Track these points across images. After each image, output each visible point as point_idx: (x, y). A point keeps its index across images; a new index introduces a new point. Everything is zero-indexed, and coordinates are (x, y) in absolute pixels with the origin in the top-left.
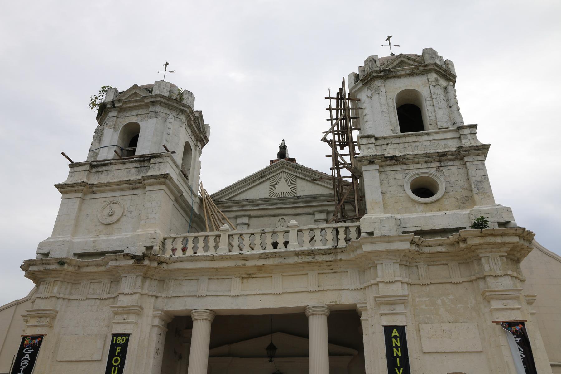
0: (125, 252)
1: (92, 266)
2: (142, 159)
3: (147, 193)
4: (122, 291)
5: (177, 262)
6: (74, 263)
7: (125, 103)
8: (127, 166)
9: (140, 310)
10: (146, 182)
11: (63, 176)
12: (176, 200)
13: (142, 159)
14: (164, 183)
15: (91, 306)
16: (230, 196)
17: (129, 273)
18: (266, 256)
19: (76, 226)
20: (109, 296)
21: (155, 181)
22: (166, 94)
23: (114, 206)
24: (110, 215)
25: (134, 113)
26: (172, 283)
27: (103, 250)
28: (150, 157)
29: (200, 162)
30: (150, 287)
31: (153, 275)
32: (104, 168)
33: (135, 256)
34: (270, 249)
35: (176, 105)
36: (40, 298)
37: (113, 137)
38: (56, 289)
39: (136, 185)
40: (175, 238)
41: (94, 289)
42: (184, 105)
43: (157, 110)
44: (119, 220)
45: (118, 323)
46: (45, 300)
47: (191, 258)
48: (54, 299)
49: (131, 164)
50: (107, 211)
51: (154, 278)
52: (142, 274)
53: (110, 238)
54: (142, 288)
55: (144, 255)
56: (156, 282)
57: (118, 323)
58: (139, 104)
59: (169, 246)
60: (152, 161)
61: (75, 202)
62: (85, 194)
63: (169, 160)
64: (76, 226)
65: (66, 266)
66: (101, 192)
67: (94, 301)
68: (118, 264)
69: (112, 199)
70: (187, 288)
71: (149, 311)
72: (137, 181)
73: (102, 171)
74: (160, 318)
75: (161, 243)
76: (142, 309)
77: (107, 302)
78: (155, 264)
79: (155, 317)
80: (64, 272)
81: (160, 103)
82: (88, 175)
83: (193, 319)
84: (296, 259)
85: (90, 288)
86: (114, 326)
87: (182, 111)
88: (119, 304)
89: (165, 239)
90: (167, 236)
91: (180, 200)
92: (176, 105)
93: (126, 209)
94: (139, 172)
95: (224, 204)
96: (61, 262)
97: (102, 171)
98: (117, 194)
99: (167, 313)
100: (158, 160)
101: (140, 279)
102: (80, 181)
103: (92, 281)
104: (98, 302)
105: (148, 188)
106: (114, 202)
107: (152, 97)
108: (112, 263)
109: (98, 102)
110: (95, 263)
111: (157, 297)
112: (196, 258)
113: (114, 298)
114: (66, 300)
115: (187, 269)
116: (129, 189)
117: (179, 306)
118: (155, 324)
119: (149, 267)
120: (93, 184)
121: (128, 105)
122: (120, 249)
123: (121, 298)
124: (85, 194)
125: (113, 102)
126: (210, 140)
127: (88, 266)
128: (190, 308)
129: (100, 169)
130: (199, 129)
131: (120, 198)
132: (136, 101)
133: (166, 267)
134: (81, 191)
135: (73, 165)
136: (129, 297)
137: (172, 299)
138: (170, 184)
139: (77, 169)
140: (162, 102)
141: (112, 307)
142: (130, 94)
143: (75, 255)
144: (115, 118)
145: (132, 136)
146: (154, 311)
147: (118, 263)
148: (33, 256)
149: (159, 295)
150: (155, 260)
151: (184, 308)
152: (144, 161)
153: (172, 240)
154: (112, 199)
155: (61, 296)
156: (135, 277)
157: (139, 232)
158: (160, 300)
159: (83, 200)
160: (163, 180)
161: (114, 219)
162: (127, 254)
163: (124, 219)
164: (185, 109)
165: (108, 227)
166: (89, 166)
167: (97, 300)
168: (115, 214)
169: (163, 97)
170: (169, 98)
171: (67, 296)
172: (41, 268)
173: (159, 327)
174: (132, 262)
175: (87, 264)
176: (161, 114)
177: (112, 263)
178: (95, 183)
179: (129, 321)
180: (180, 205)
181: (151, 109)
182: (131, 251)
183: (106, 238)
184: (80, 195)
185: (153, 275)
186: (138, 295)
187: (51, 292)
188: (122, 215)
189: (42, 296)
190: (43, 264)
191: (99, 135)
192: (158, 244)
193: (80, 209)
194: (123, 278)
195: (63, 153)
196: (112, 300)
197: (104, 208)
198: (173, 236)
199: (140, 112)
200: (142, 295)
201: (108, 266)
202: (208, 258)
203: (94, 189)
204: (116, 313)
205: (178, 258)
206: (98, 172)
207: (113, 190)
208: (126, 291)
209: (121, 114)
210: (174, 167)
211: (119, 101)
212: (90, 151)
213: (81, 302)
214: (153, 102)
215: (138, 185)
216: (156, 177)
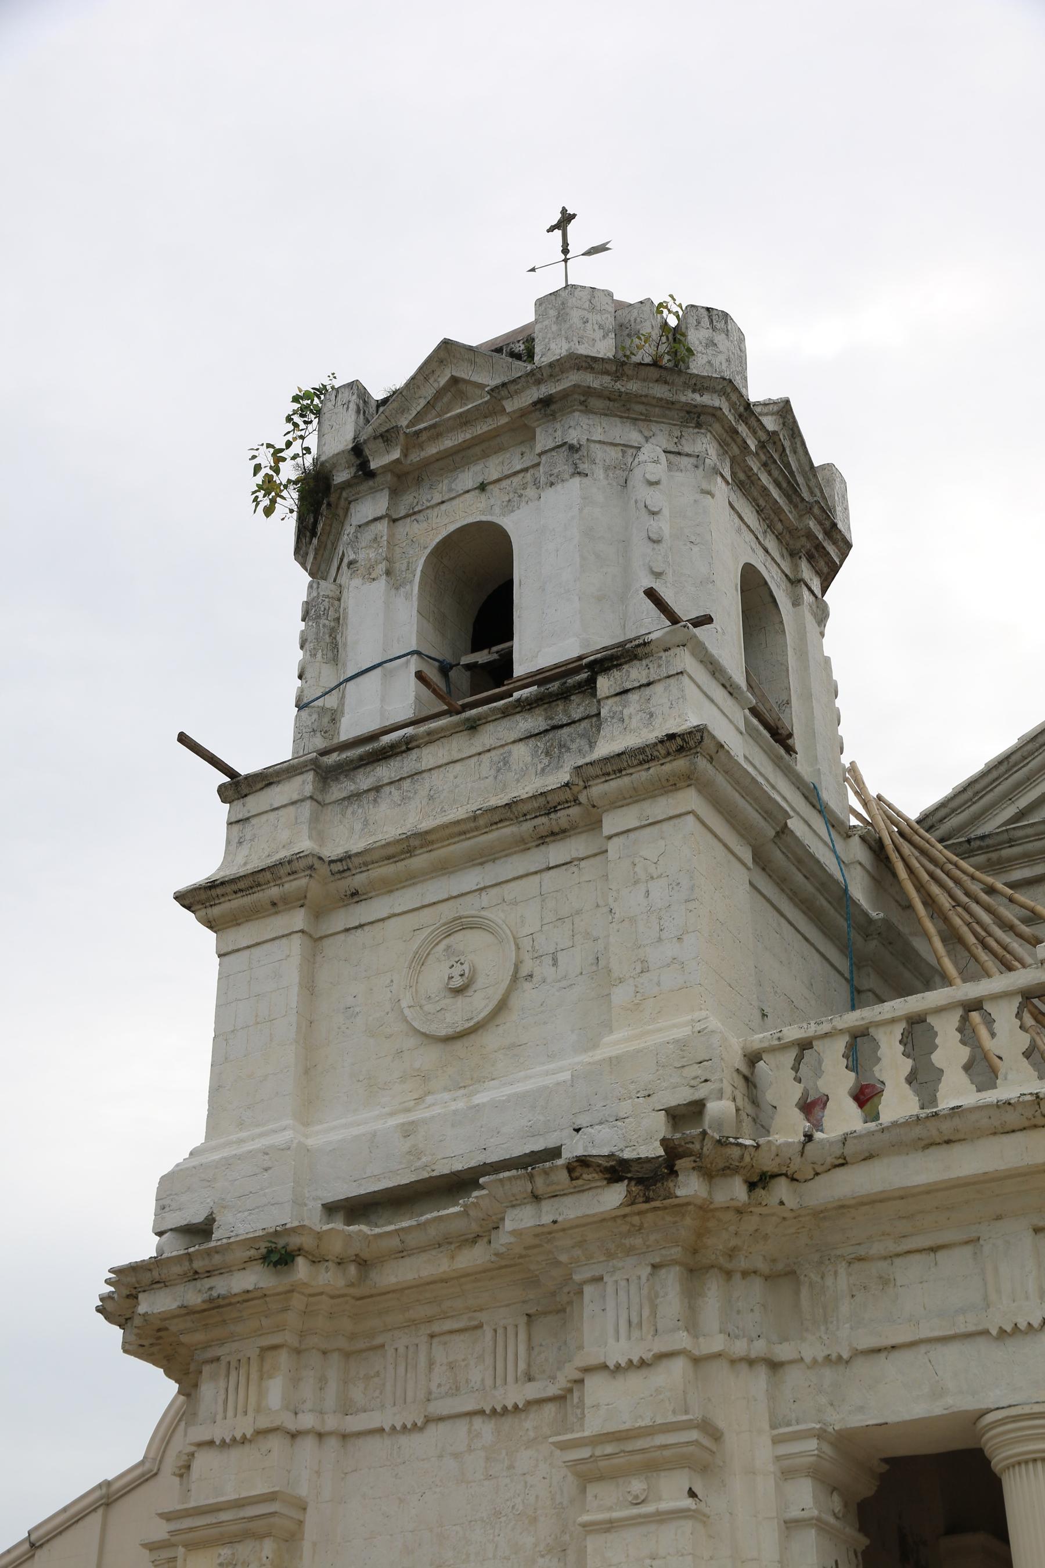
0: (567, 1155)
1: (422, 1249)
2: (554, 686)
3: (613, 846)
4: (592, 1355)
5: (843, 1163)
6: (336, 1247)
7: (414, 440)
8: (488, 736)
9: (706, 1442)
10: (598, 790)
11: (205, 851)
12: (761, 861)
13: (554, 686)
14: (688, 779)
15: (456, 1456)
16: (1023, 802)
17: (610, 1255)
19: (306, 1072)
20: (532, 1391)
21: (642, 776)
22: (604, 348)
23: (470, 941)
24: (459, 991)
25: (467, 479)
26: (841, 1280)
27: (458, 1166)
28: (591, 666)
29: (827, 661)
30: (729, 1316)
31: (732, 1253)
32: (384, 772)
33: (625, 1163)
35: (659, 391)
36: (211, 1443)
37: (392, 618)
38: (275, 1391)
39: (552, 820)
40: (804, 1046)
41: (451, 1366)
42: (701, 384)
43: (573, 436)
44: (502, 1006)
45: (609, 1526)
46: (235, 1453)
47: (917, 1131)
48: (275, 1443)
49: (506, 723)
50: (437, 974)
51: (743, 1264)
52: (676, 1252)
53: (481, 1098)
54: (691, 1324)
55: (673, 1152)
56: (757, 1285)
57: (609, 1526)
58: (482, 428)
59: (782, 1087)
60: (604, 684)
61: (280, 957)
62: (318, 914)
63: (685, 660)
64: (309, 1070)
65: (302, 1268)
67: (462, 1426)
68: (547, 1219)
69: (448, 911)
70: (926, 1294)
71: (752, 1446)
72: (554, 799)
73: (377, 789)
74: (816, 1474)
75: (740, 1082)
76: (716, 1435)
77: (529, 1423)
78: (736, 1190)
79: (787, 1473)
80: (297, 1302)
81: (583, 399)
82: (314, 819)
83: (997, 1463)
85: (431, 1364)
86: (592, 1543)
87: (696, 418)
88: (593, 1426)
89: (753, 1058)
90: (759, 1039)
91: (778, 856)
92: (659, 391)
93: (526, 943)
94: (553, 755)
95: (997, 847)
96: (278, 1253)
97: (377, 789)
98: (470, 879)
99: (844, 1442)
100: (635, 673)
101: (671, 1281)
102: (283, 854)
103: (436, 1328)
104: (486, 1428)
105: (611, 823)
106: (461, 925)
107: (536, 377)
108: (521, 1219)
109: (288, 472)
110: (432, 1232)
111: (775, 1366)
112: (947, 1127)
113: (560, 1399)
114: (333, 1442)
115: (905, 1195)
116: (522, 845)
117: (905, 1399)
118: (795, 1513)
119: (705, 1209)
120: (348, 857)
121: (432, 450)
122: (538, 1145)
123: (599, 1391)
124: (318, 914)
125: (357, 449)
126: (855, 540)
127: (402, 1253)
128: (969, 1404)
129: (364, 780)
130: (791, 492)
131: (485, 899)
132: (465, 421)
133: (791, 1202)
134: (300, 900)
135: (237, 787)
136: (634, 1381)
137: (861, 1366)
138: (720, 780)
139: (257, 802)
140: (589, 392)
141: (563, 1446)
142: (428, 392)
143: (331, 1209)
144: (382, 527)
145: (479, 596)
146: (776, 1441)
147: (548, 1213)
148: (143, 1246)
149: (784, 1352)
150: (729, 1170)
151: (937, 1409)
152: (564, 695)
153: (791, 1056)
154: (448, 911)
155: (307, 1421)
156: (649, 1269)
157: (616, 1042)
158: (794, 1377)
159: (315, 940)
160: (680, 764)
161: (479, 1003)
162: (583, 1162)
163: (527, 996)
165: (458, 1046)
166: (310, 776)
167: (478, 1422)
168: (480, 982)
169: (589, 363)
170: (620, 366)
171: (331, 1423)
172: (193, 1296)
173: (819, 1524)
174: (614, 1196)
175: (395, 1242)
176: (599, 453)
177: (521, 1219)
178: (357, 845)
179: (664, 1506)
180: (782, 882)
181: (544, 440)
182: (602, 1142)
183: (460, 1105)
184: (298, 919)
185: (732, 1253)
186: (678, 1367)
187: (258, 1410)
188: (515, 978)
189: (218, 1432)
190: (195, 1276)
191: (324, 627)
192: (728, 1090)
193: (309, 987)
194: (588, 1290)
195: (183, 739)
196: (550, 1410)
197: (420, 960)
198: (793, 1033)
199: (492, 468)
200: (697, 1361)
201: (502, 1240)
202: (1012, 1118)
203: (358, 880)
204: (587, 1476)
205: (845, 1140)
206: (355, 797)
207: (444, 869)
208: (618, 1352)
209: (408, 500)
210: (719, 694)
211: (386, 437)
212: (301, 705)
213: (403, 1440)
214: (545, 403)
215: (562, 818)
216: (643, 756)
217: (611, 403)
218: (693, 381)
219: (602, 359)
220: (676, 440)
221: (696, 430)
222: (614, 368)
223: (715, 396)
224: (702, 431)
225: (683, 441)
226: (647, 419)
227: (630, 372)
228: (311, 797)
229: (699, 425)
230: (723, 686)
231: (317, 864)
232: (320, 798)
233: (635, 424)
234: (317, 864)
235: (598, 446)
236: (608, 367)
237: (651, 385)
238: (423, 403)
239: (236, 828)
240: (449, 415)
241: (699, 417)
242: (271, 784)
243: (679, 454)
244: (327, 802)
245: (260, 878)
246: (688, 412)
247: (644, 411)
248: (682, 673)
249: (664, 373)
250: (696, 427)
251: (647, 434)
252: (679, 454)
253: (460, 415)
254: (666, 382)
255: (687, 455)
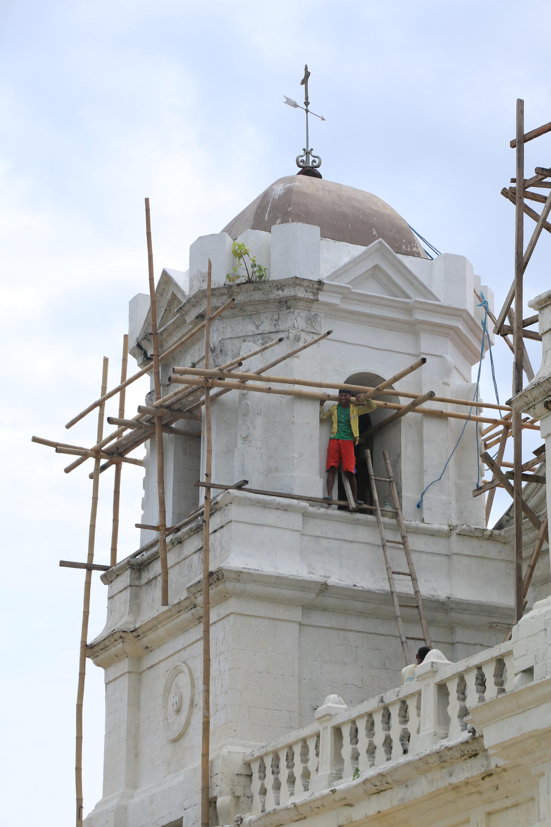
14: (225, 597)
18: (379, 786)
34: (383, 765)
42: (280, 285)
66: (161, 642)
84: (441, 780)
92: (258, 296)
106: (177, 671)
164: (287, 292)
184: (124, 666)
195: (63, 564)
207: (173, 635)
217: (233, 310)
218: (275, 284)
219: (218, 288)
220: (275, 322)
221: (287, 311)
222: (227, 291)
223: (291, 288)
224: (292, 310)
225: (280, 322)
226: (257, 313)
227: (237, 290)
228: (131, 586)
229: (289, 308)
230: (277, 509)
231: (123, 635)
232: (137, 583)
233: (251, 318)
234: (123, 635)
235: (229, 341)
236: (223, 291)
237: (252, 293)
238: (163, 310)
239: (111, 600)
240: (169, 323)
241: (286, 303)
242: (118, 575)
243: (277, 332)
244: (142, 584)
245: (107, 642)
246: (279, 302)
247: (253, 309)
248: (231, 521)
249: (256, 285)
250: (287, 309)
251: (257, 323)
252: (277, 332)
253: (173, 323)
254: (259, 289)
255: (282, 331)
